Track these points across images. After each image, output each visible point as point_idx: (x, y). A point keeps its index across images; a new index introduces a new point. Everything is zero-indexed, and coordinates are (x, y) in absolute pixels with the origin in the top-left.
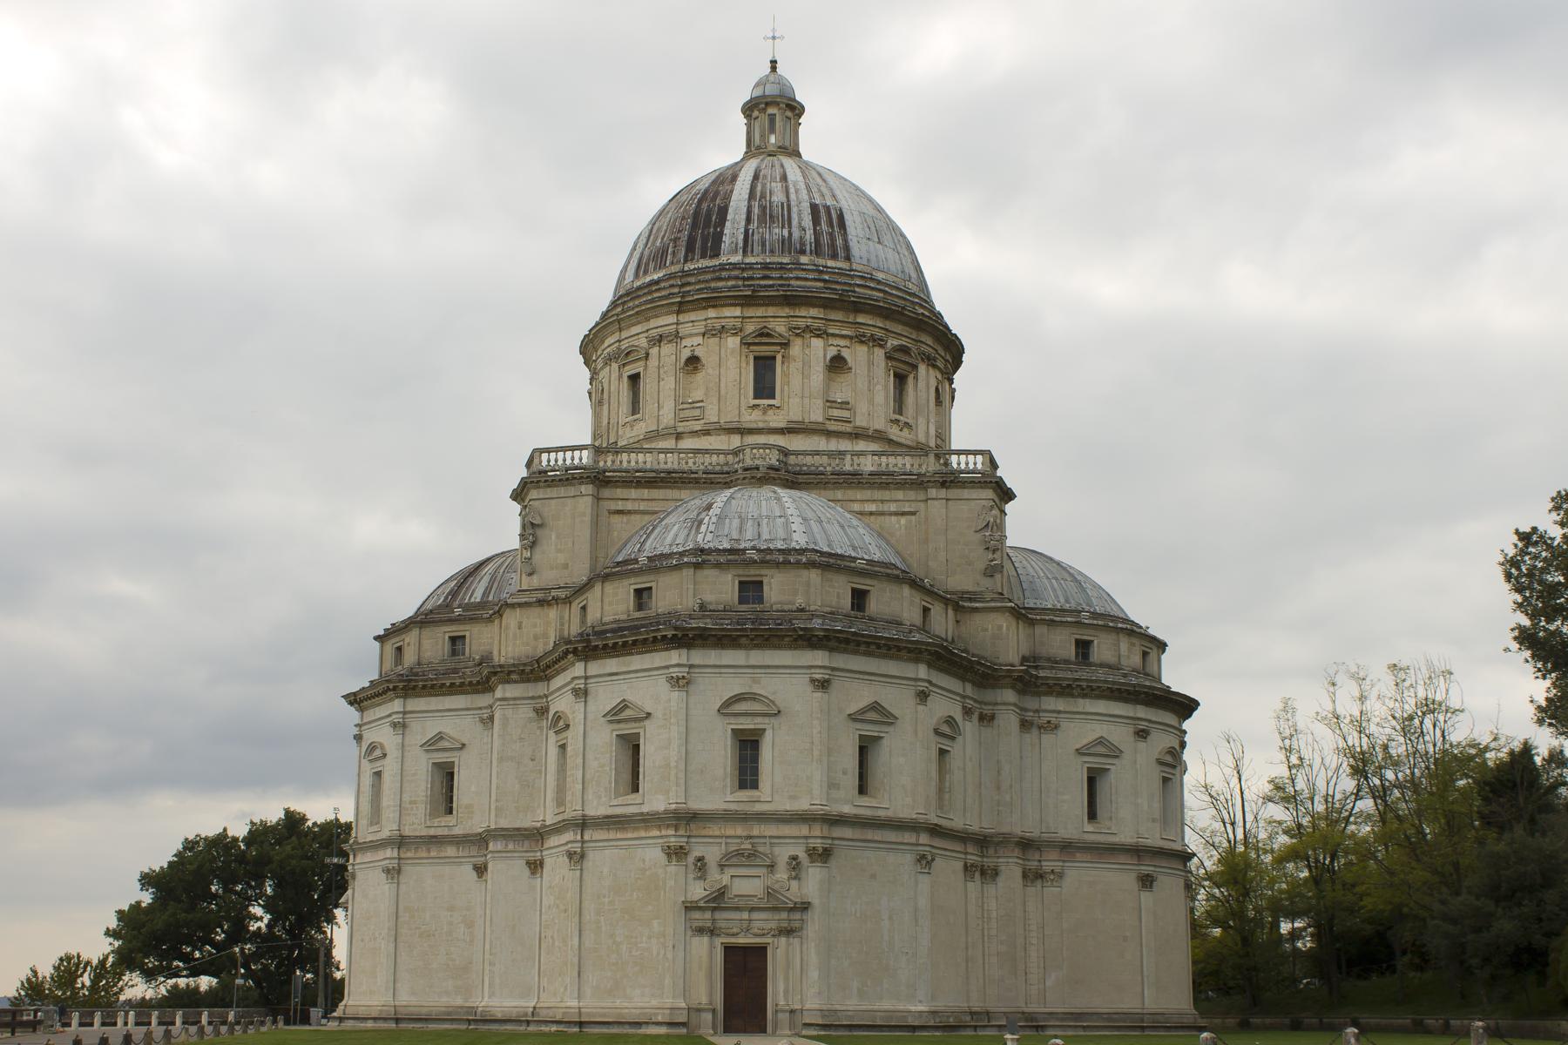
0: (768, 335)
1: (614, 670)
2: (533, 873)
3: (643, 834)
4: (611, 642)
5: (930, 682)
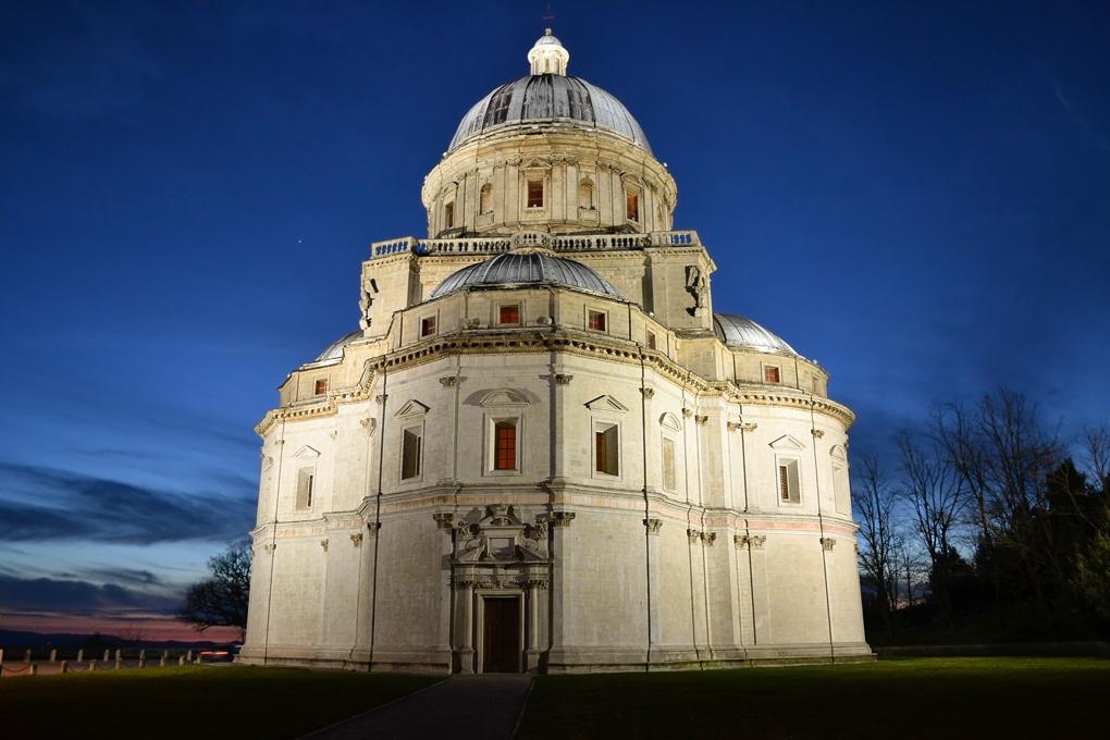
0: (537, 165)
1: (404, 378)
2: (356, 545)
3: (420, 506)
4: (400, 357)
5: (655, 384)
